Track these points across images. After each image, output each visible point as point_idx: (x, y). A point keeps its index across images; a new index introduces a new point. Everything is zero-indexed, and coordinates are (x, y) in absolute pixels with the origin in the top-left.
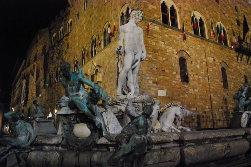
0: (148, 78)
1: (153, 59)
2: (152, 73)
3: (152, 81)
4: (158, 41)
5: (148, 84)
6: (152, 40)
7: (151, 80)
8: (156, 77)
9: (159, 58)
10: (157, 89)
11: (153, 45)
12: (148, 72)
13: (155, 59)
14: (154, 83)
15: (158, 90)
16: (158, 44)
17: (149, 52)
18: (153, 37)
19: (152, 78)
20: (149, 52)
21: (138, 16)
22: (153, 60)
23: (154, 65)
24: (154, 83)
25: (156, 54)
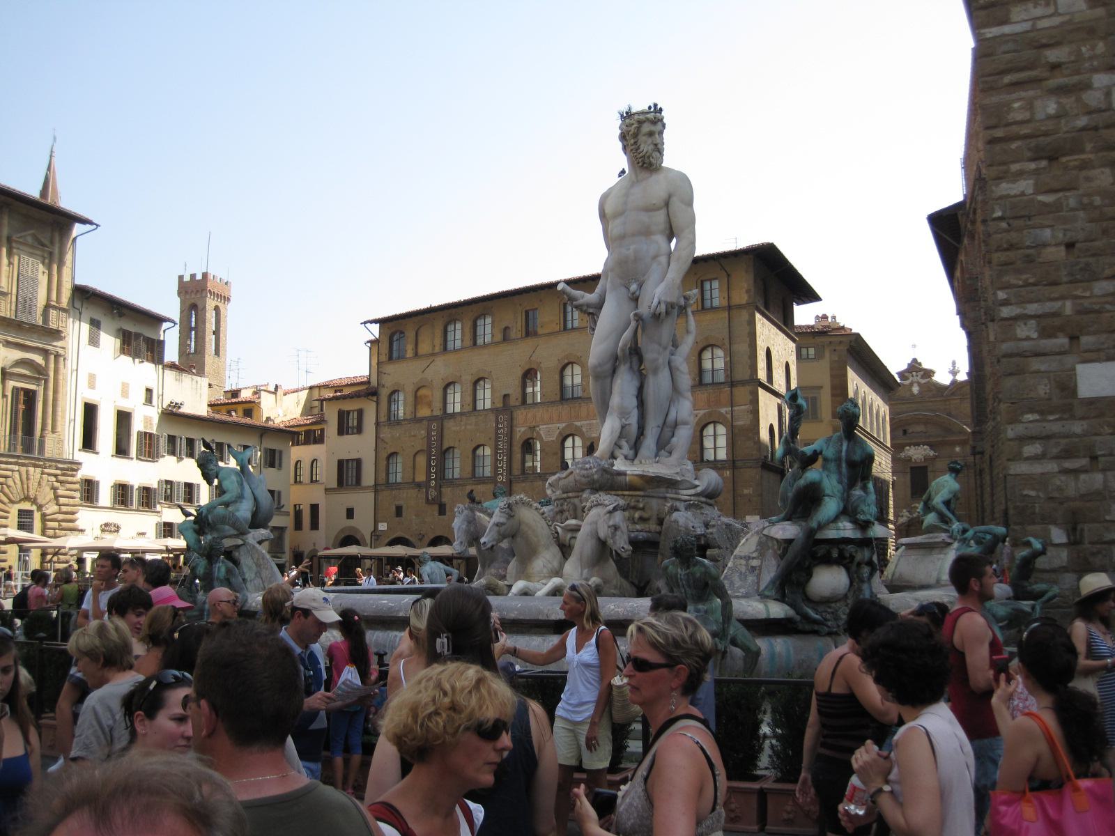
0: (1006, 312)
1: (1040, 198)
2: (1031, 281)
3: (1033, 322)
4: (1076, 79)
5: (1006, 347)
6: (1031, 93)
7: (1024, 318)
8: (1062, 298)
9: (1088, 179)
10: (1069, 360)
11: (1040, 115)
12: (1006, 279)
13: (1061, 194)
14: (1046, 333)
15: (1081, 369)
16: (1079, 100)
17: (1015, 167)
18: (1033, 74)
19: (1033, 308)
20: (1015, 167)
21: (632, 141)
22: (1045, 204)
23: (1047, 233)
24: (1046, 333)
25: (1064, 159)
